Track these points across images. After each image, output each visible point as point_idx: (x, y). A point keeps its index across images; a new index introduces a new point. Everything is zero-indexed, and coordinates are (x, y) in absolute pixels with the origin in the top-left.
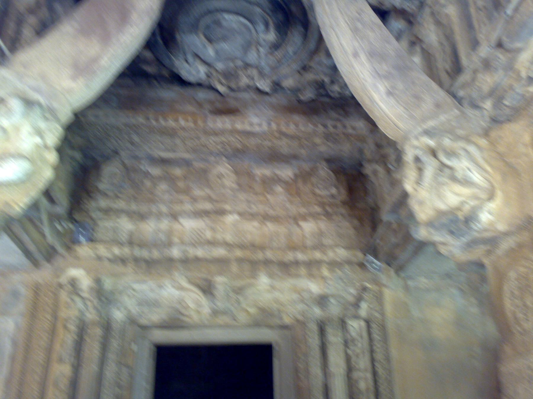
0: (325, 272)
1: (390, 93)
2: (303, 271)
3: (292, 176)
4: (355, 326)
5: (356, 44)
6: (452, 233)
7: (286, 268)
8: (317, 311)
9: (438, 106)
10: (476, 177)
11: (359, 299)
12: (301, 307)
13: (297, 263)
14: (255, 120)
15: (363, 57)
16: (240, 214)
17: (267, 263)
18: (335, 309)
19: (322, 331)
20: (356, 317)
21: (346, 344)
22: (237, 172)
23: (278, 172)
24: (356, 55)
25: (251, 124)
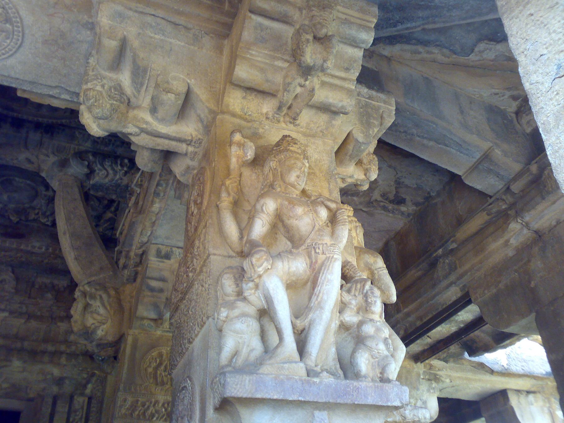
0: (63, 360)
1: (76, 259)
2: (46, 358)
3: (65, 285)
4: (80, 401)
5: (66, 227)
6: (86, 339)
7: (34, 355)
8: (55, 389)
9: (101, 269)
10: (102, 311)
11: (88, 382)
12: (42, 385)
13: (44, 352)
14: (37, 244)
15: (68, 235)
16: (11, 312)
17: (21, 350)
18: (68, 388)
19: (54, 404)
20: (82, 394)
21: (69, 414)
22: (17, 279)
23: (56, 282)
24: (65, 233)
25: (34, 247)
